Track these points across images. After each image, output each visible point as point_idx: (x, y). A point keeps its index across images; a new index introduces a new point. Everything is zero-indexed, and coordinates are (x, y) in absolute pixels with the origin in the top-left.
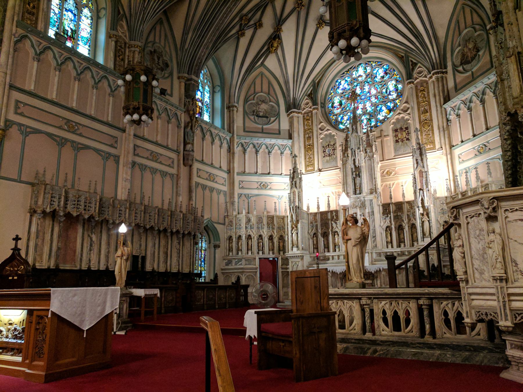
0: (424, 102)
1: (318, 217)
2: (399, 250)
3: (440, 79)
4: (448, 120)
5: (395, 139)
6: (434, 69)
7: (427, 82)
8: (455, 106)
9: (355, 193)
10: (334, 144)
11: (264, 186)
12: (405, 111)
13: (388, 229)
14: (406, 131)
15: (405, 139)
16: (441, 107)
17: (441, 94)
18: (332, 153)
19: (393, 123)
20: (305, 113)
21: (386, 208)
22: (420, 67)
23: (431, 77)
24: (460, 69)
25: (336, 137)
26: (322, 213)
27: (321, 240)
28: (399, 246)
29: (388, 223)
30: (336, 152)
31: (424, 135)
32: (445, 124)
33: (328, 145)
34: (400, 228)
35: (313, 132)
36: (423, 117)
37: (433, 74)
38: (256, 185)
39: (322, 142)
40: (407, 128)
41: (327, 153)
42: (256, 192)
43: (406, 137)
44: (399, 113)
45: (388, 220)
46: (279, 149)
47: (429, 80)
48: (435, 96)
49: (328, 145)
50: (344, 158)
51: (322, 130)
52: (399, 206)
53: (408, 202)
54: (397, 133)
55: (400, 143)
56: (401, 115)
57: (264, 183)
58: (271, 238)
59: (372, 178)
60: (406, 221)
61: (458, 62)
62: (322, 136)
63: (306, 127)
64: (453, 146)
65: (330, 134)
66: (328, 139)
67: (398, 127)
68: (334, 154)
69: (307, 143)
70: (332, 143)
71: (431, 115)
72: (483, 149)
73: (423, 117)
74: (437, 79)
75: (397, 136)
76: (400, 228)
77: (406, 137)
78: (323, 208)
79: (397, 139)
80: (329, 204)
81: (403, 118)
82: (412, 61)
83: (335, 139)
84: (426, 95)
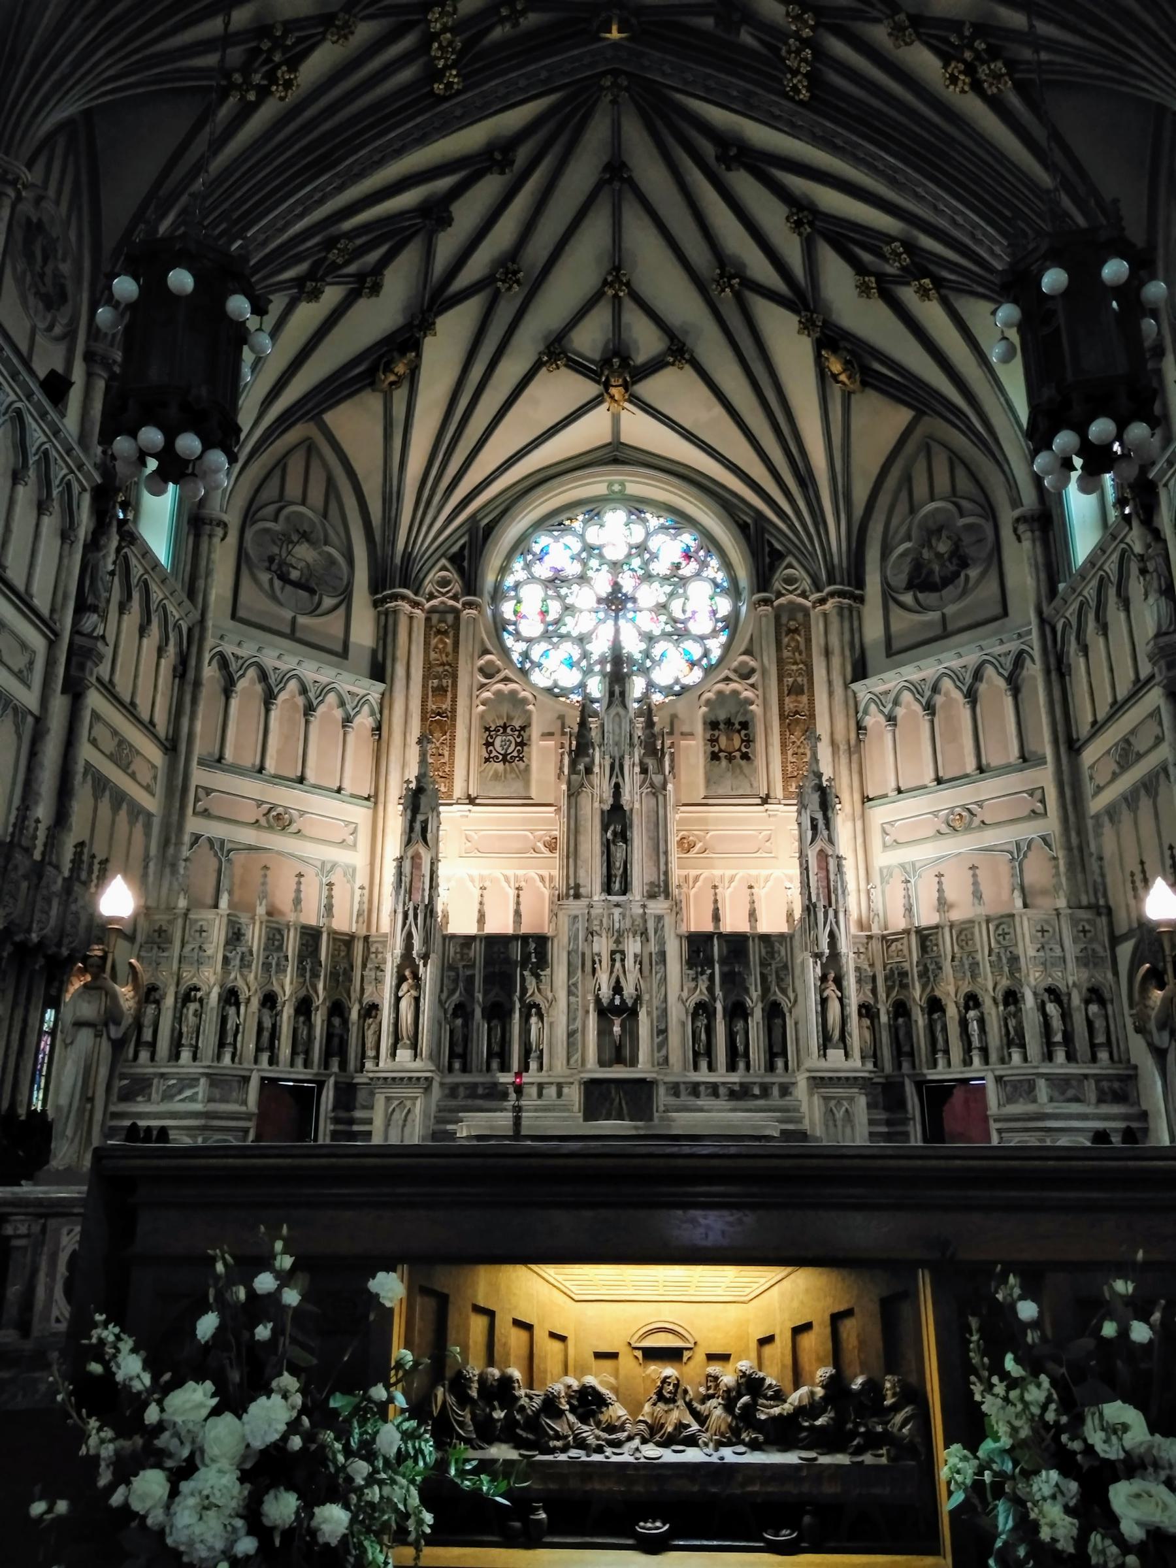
0: (795, 663)
2: (734, 1078)
3: (846, 613)
4: (860, 727)
5: (709, 749)
6: (831, 581)
7: (806, 612)
8: (887, 693)
9: (608, 889)
10: (523, 728)
12: (745, 674)
13: (703, 1010)
14: (743, 732)
15: (738, 754)
16: (846, 686)
17: (847, 653)
18: (515, 754)
19: (708, 702)
20: (433, 610)
22: (790, 566)
23: (822, 601)
24: (908, 598)
25: (531, 707)
28: (732, 1067)
29: (702, 994)
30: (529, 753)
31: (790, 753)
32: (853, 735)
33: (505, 727)
34: (737, 1012)
35: (455, 677)
37: (832, 594)
38: (251, 813)
39: (484, 711)
40: (745, 725)
41: (499, 750)
42: (248, 836)
43: (739, 750)
44: (727, 679)
45: (703, 985)
46: (342, 704)
47: (814, 607)
48: (827, 653)
49: (505, 727)
50: (574, 777)
51: (488, 676)
52: (737, 944)
53: (766, 939)
54: (716, 733)
55: (724, 763)
56: (733, 686)
57: (280, 810)
59: (659, 850)
60: (755, 994)
61: (900, 579)
62: (487, 695)
63: (433, 655)
64: (870, 800)
65: (513, 693)
66: (505, 709)
67: (722, 716)
68: (521, 759)
69: (432, 706)
70: (517, 724)
71: (811, 702)
74: (840, 609)
75: (717, 740)
76: (737, 1012)
77: (739, 750)
78: (500, 923)
79: (716, 749)
80: (518, 914)
81: (735, 693)
82: (770, 545)
83: (528, 714)
84: (802, 647)
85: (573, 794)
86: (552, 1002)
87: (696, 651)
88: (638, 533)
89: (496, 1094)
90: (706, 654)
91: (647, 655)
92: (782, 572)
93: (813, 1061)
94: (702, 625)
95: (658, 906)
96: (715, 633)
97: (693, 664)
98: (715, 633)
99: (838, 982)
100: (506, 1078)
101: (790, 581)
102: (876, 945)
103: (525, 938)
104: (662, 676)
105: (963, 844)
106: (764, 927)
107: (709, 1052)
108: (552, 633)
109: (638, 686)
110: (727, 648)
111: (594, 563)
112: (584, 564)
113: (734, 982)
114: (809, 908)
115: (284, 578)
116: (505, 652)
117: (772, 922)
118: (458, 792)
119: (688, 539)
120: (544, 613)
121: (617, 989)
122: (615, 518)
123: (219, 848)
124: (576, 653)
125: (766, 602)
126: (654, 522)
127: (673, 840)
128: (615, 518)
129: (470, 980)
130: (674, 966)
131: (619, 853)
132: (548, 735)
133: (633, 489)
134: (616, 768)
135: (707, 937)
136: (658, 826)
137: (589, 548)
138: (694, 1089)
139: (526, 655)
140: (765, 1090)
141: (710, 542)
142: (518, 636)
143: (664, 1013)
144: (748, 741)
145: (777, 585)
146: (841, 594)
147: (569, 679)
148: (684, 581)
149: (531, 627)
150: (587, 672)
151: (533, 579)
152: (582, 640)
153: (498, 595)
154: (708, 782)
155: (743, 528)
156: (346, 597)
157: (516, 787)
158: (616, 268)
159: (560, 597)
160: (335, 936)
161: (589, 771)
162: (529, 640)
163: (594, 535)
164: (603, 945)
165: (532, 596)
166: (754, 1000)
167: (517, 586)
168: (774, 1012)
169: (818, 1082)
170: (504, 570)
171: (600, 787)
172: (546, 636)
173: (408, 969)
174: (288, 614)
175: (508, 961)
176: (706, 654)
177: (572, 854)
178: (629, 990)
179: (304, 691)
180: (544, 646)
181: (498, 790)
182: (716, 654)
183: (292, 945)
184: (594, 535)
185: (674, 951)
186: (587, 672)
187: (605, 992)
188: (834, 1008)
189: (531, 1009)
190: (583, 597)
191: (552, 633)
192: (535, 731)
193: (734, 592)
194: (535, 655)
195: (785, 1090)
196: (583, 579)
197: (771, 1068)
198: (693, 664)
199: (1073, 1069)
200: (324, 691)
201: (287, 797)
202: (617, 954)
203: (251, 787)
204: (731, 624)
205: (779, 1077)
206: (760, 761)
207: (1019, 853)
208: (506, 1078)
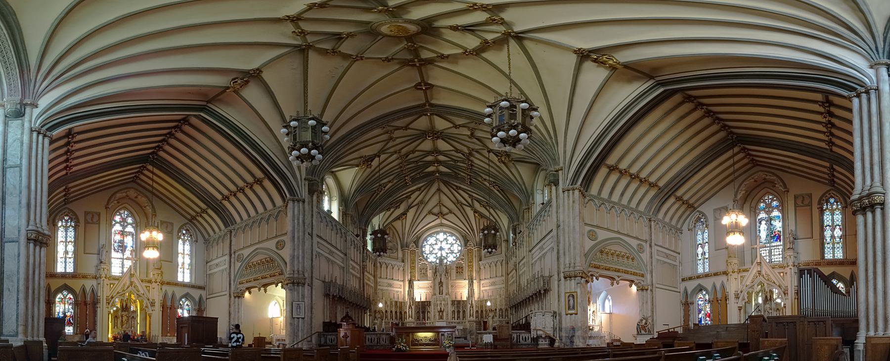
1: (420, 303)
12: (462, 259)
13: (454, 311)
28: (458, 319)
29: (453, 309)
34: (459, 312)
42: (386, 288)
52: (459, 302)
53: (463, 301)
59: (447, 288)
67: (458, 266)
73: (469, 264)
76: (459, 312)
86: (432, 311)
88: (445, 236)
90: (457, 256)
91: (447, 256)
95: (447, 296)
96: (458, 252)
97: (454, 257)
98: (458, 252)
101: (470, 245)
102: (479, 302)
103: (427, 302)
104: (449, 259)
106: (463, 299)
107: (454, 317)
108: (431, 253)
109: (445, 261)
111: (438, 241)
116: (424, 256)
117: (465, 298)
118: (416, 279)
121: (441, 309)
122: (442, 234)
126: (448, 235)
129: (419, 308)
133: (444, 230)
136: (447, 284)
137: (437, 239)
139: (427, 256)
141: (457, 238)
142: (425, 254)
143: (448, 312)
144: (462, 270)
145: (468, 245)
146: (478, 248)
148: (453, 244)
149: (427, 252)
150: (437, 259)
153: (422, 247)
154: (456, 276)
160: (399, 302)
162: (427, 254)
168: (464, 312)
169: (469, 321)
170: (423, 243)
172: (430, 253)
173: (410, 307)
176: (457, 256)
177: (434, 289)
178: (442, 309)
180: (429, 255)
181: (423, 278)
182: (458, 256)
183: (394, 304)
184: (438, 237)
185: (450, 303)
188: (472, 311)
189: (428, 312)
191: (431, 253)
193: (461, 246)
194: (428, 256)
196: (436, 244)
198: (454, 257)
199: (503, 319)
200: (395, 265)
202: (441, 304)
204: (460, 251)
205: (464, 321)
206: (464, 273)
207: (501, 288)
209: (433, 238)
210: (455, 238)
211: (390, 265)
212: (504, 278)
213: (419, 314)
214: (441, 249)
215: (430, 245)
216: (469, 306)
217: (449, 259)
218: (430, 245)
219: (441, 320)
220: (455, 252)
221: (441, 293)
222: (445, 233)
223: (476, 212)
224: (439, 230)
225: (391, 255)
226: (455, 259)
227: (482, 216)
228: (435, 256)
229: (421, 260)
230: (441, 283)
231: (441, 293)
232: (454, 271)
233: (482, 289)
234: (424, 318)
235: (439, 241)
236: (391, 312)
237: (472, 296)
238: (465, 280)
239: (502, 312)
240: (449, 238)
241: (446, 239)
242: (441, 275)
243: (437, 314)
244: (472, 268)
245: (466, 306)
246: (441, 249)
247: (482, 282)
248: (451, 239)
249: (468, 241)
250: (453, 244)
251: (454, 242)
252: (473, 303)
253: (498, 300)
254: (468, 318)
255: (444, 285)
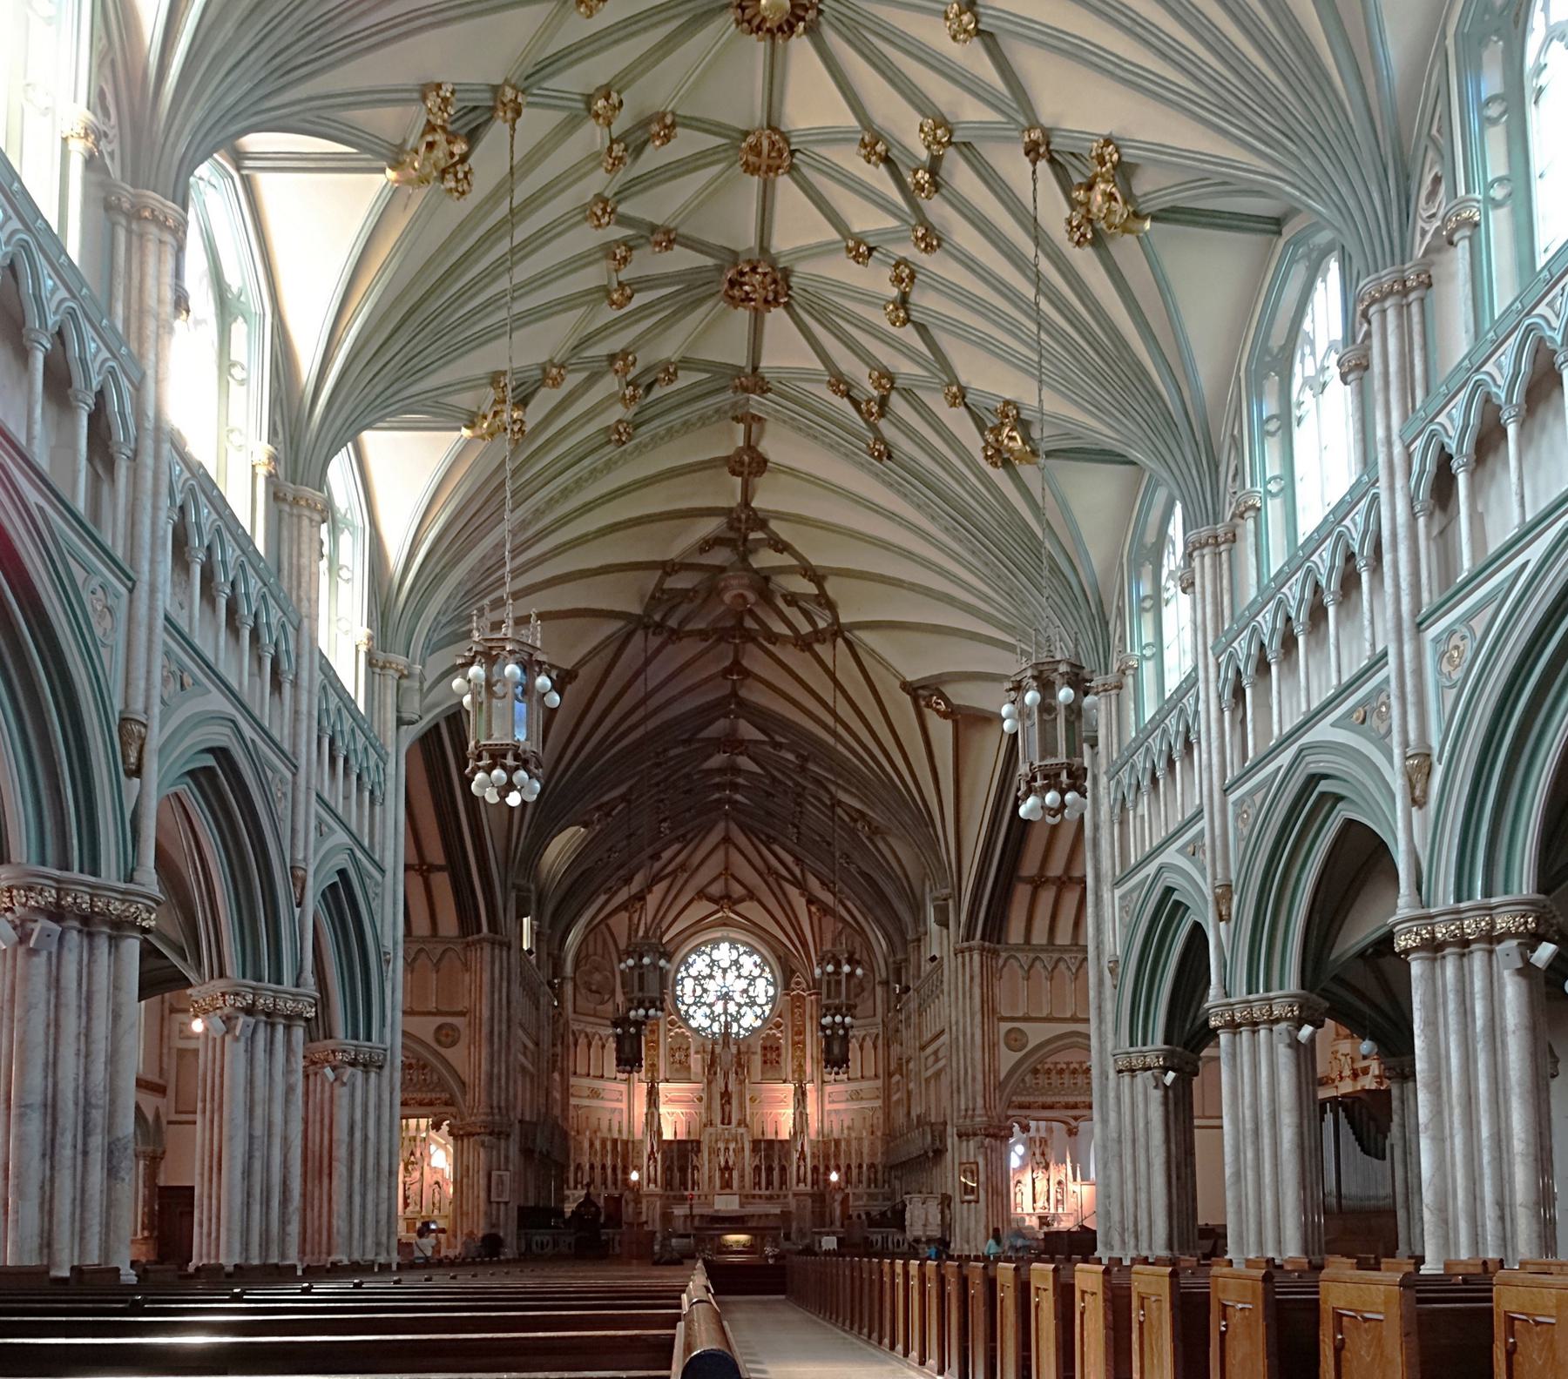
1: (675, 1146)
2: (768, 1193)
7: (804, 997)
9: (723, 1123)
11: (595, 1094)
12: (778, 1026)
13: (757, 1169)
21: (756, 1143)
26: (679, 1142)
27: (677, 1175)
28: (767, 1189)
29: (757, 1162)
34: (770, 1170)
36: (796, 1038)
38: (587, 1093)
40: (778, 1049)
42: (586, 1102)
48: (811, 1018)
52: (770, 1143)
53: (781, 1141)
58: (614, 1168)
59: (742, 1106)
60: (776, 1162)
66: (679, 1040)
67: (768, 1044)
72: (856, 1096)
73: (796, 1038)
76: (770, 1170)
78: (682, 1136)
85: (709, 1083)
86: (703, 1165)
87: (759, 1012)
89: (683, 1199)
91: (738, 1012)
92: (795, 979)
93: (794, 1188)
94: (762, 1000)
95: (742, 1130)
96: (767, 1004)
98: (767, 1004)
99: (804, 1160)
100: (686, 1193)
101: (798, 983)
102: (821, 1145)
103: (692, 1141)
104: (745, 1022)
105: (855, 1105)
106: (781, 1137)
107: (759, 1183)
108: (698, 1003)
109: (735, 1028)
110: (771, 1010)
111: (715, 968)
112: (711, 968)
113: (768, 1157)
114: (795, 1133)
115: (591, 991)
117: (785, 1135)
118: (661, 1077)
119: (756, 958)
120: (694, 991)
121: (727, 1162)
122: (725, 946)
123: (577, 1107)
124: (708, 1012)
125: (788, 995)
126: (742, 950)
127: (748, 1097)
128: (725, 946)
129: (672, 1158)
130: (747, 1153)
131: (727, 1108)
132: (697, 1053)
133: (732, 935)
134: (726, 1075)
135: (760, 1141)
136: (741, 1095)
138: (754, 1196)
139: (687, 1012)
140: (778, 1196)
142: (683, 1003)
143: (743, 1169)
144: (779, 1055)
145: (793, 986)
147: (705, 1024)
148: (755, 978)
149: (689, 1000)
150: (713, 1020)
151: (689, 976)
152: (711, 1006)
154: (763, 1073)
155: (779, 958)
156: (613, 993)
157: (684, 1075)
158: (726, 869)
159: (702, 985)
160: (622, 1141)
161: (715, 1073)
162: (689, 1006)
163: (716, 955)
164: (721, 1145)
165: (689, 983)
166: (776, 1165)
167: (683, 978)
168: (783, 1169)
171: (719, 1085)
174: (592, 1006)
175: (686, 1150)
177: (709, 1108)
178: (731, 1163)
179: (601, 1039)
180: (694, 1008)
181: (677, 1076)
184: (716, 955)
185: (747, 1146)
186: (713, 1020)
187: (723, 1163)
188: (802, 1168)
189: (695, 1168)
190: (711, 985)
192: (692, 1051)
193: (774, 984)
194: (691, 1012)
195: (786, 1196)
196: (711, 977)
197: (781, 1188)
198: (757, 1017)
199: (876, 1191)
201: (598, 1084)
202: (727, 1149)
203: (586, 1082)
204: (773, 999)
206: (782, 1064)
208: (686, 1193)
209: (704, 957)
210: (759, 961)
211: (597, 1037)
212: (879, 1083)
213: (672, 1171)
214: (726, 997)
215: (695, 978)
216: (795, 1156)
217: (745, 1022)
218: (695, 978)
219: (728, 1191)
220: (759, 1001)
221: (727, 1120)
222: (733, 944)
223: (811, 900)
224: (718, 935)
225: (599, 1007)
226: (758, 1023)
227: (826, 910)
228: (708, 1012)
229: (672, 1023)
230: (726, 1096)
231: (727, 1120)
232: (757, 1060)
233: (828, 1107)
234: (684, 1184)
235: (719, 967)
236: (604, 1167)
237: (802, 1132)
238: (785, 1082)
239: (876, 1173)
240: (744, 960)
241: (736, 962)
242: (726, 1075)
243: (717, 1174)
244: (803, 1050)
245: (788, 1154)
246: (726, 997)
247: (828, 1089)
248: (748, 963)
249: (793, 972)
250: (755, 978)
251: (757, 972)
252: (806, 1148)
253: (866, 1143)
254: (794, 1188)
255: (735, 1102)
